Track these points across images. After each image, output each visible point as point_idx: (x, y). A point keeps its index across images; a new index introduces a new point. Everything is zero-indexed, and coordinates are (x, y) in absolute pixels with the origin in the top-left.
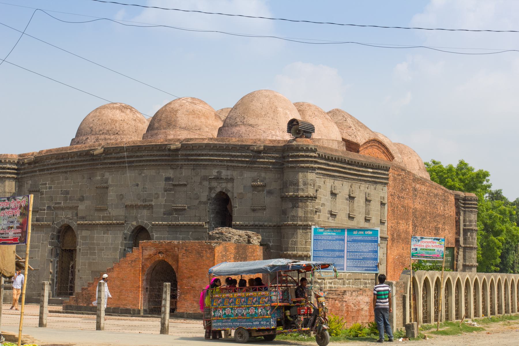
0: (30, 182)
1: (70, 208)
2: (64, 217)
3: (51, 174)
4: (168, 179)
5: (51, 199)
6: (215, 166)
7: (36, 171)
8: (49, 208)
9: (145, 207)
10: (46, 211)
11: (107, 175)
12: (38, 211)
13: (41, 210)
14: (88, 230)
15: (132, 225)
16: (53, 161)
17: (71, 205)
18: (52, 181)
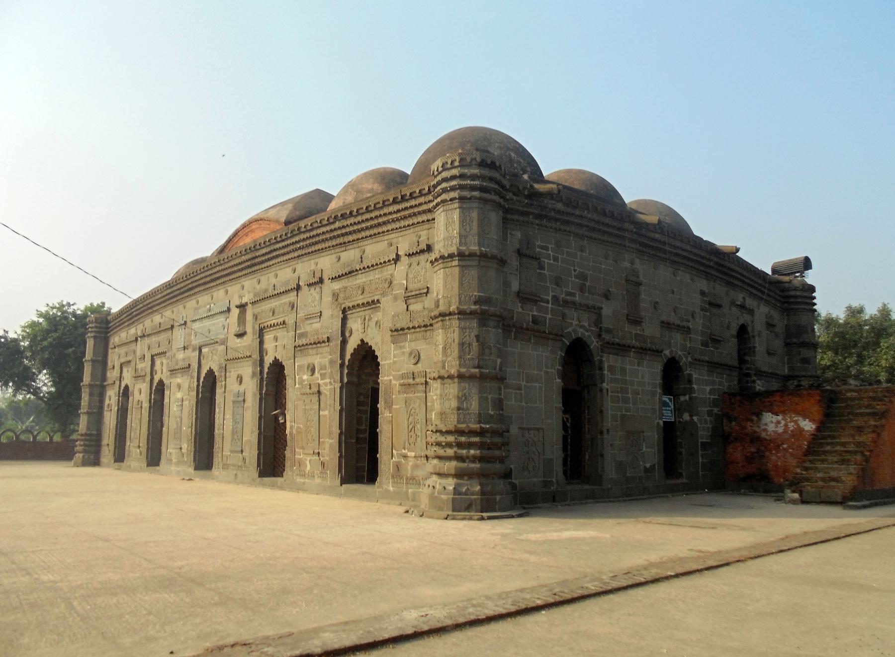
0: (518, 235)
1: (588, 308)
2: (578, 325)
3: (558, 230)
4: (703, 293)
5: (558, 282)
6: (742, 289)
7: (527, 214)
8: (555, 299)
9: (679, 328)
10: (550, 306)
11: (637, 261)
12: (536, 301)
13: (542, 300)
14: (617, 354)
15: (665, 355)
16: (560, 206)
17: (591, 303)
18: (558, 244)
